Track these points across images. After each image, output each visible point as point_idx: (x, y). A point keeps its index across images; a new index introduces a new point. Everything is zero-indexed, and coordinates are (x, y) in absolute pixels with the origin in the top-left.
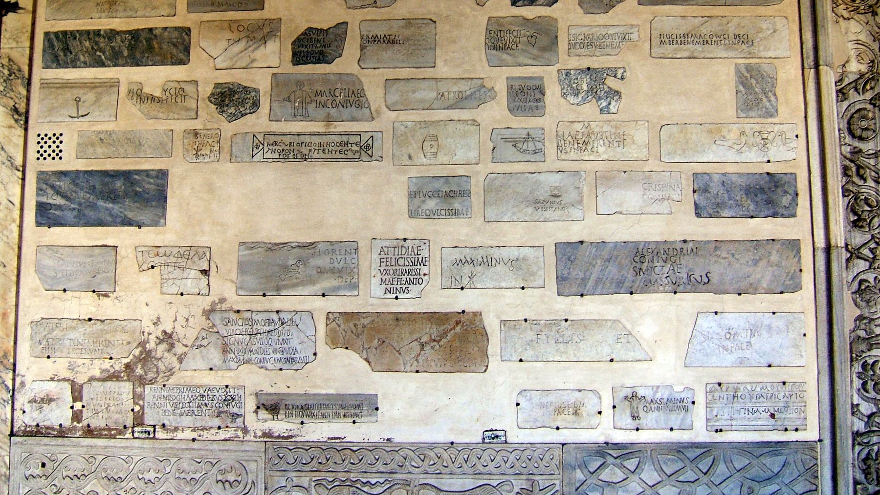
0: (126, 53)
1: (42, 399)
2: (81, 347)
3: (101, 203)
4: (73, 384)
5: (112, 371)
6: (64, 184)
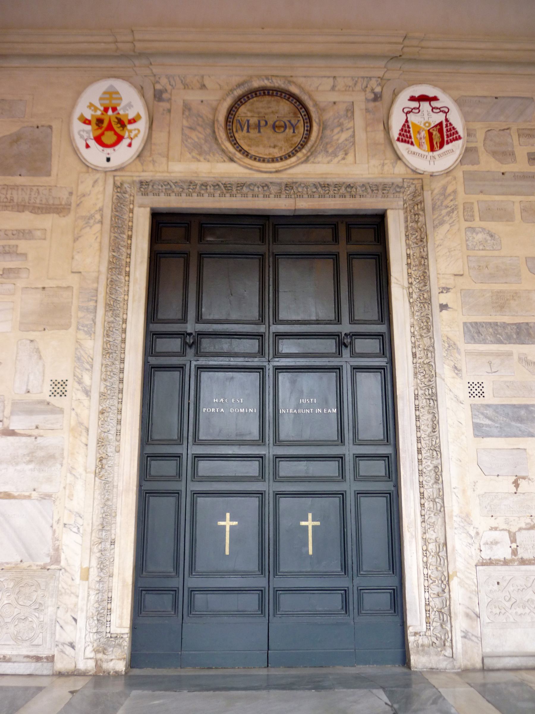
0: (515, 336)
1: (492, 543)
2: (512, 510)
3: (513, 423)
4: (509, 532)
5: (532, 524)
6: (490, 412)
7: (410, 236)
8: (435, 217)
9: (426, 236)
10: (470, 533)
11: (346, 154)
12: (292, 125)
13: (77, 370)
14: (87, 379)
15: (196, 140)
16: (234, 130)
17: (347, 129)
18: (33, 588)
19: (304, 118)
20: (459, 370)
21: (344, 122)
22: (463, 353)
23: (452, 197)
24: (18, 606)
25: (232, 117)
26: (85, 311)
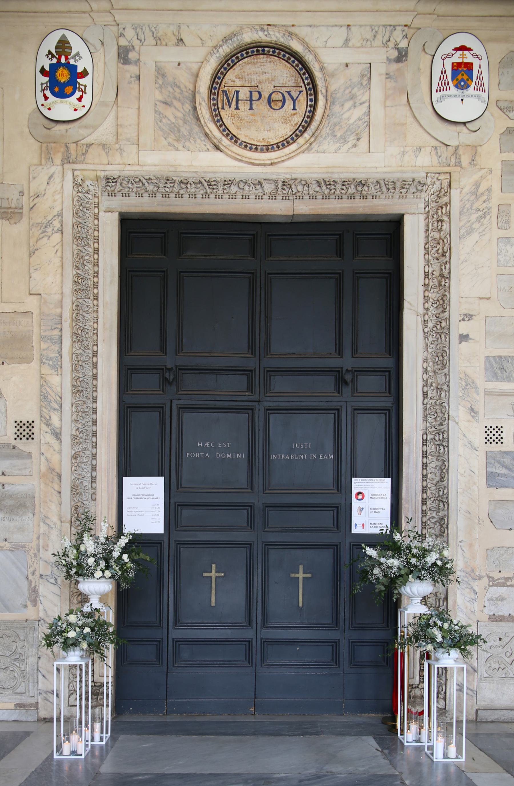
7: (430, 249)
8: (462, 224)
9: (450, 249)
10: (474, 588)
11: (358, 139)
12: (292, 98)
13: (44, 410)
14: (55, 420)
15: (173, 120)
16: (220, 106)
17: (361, 104)
19: (308, 87)
20: (476, 413)
21: (358, 94)
22: (482, 394)
23: (484, 198)
25: (218, 86)
26: (49, 341)
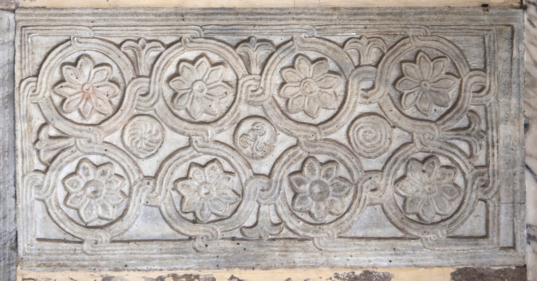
18: (445, 65)
24: (405, 123)
